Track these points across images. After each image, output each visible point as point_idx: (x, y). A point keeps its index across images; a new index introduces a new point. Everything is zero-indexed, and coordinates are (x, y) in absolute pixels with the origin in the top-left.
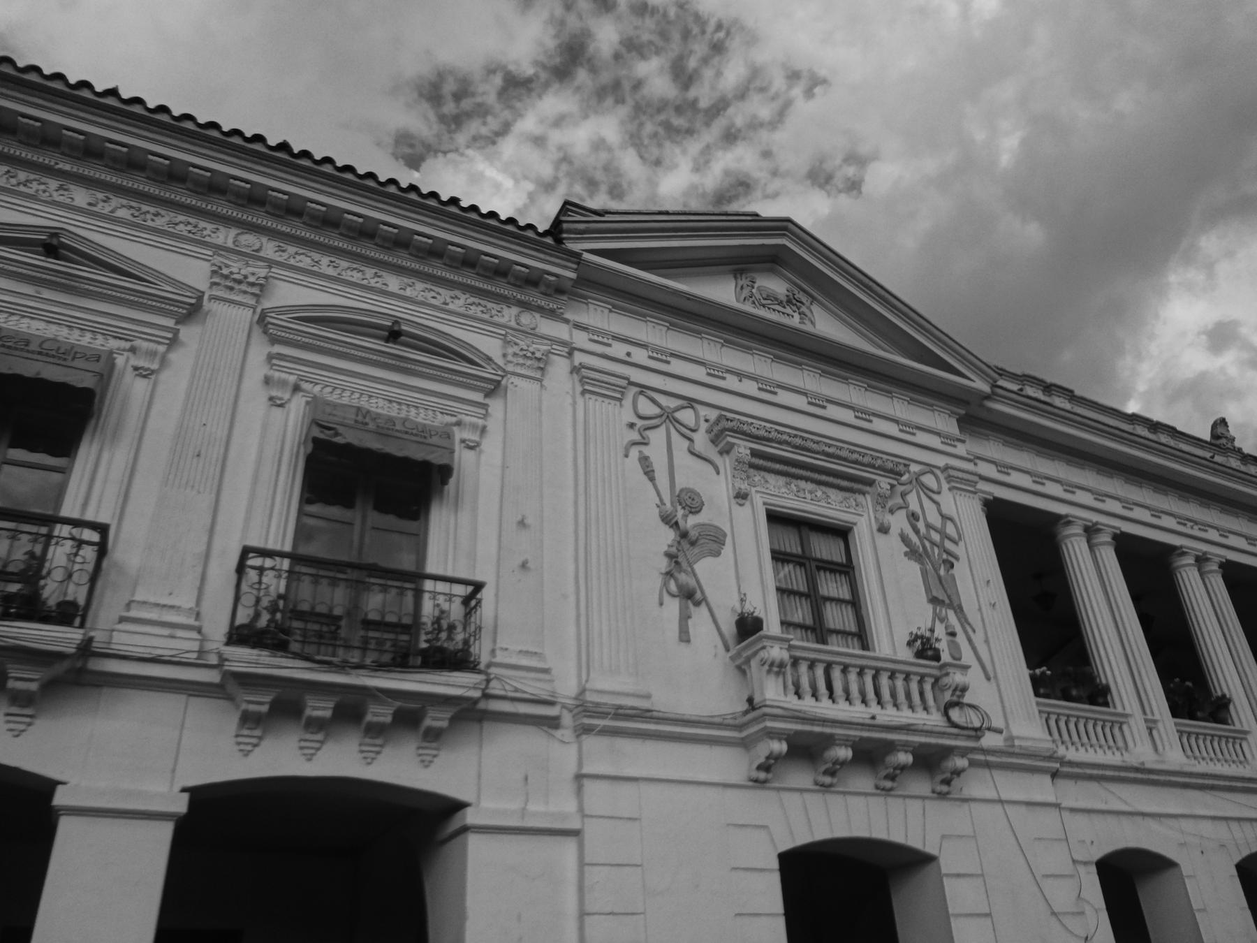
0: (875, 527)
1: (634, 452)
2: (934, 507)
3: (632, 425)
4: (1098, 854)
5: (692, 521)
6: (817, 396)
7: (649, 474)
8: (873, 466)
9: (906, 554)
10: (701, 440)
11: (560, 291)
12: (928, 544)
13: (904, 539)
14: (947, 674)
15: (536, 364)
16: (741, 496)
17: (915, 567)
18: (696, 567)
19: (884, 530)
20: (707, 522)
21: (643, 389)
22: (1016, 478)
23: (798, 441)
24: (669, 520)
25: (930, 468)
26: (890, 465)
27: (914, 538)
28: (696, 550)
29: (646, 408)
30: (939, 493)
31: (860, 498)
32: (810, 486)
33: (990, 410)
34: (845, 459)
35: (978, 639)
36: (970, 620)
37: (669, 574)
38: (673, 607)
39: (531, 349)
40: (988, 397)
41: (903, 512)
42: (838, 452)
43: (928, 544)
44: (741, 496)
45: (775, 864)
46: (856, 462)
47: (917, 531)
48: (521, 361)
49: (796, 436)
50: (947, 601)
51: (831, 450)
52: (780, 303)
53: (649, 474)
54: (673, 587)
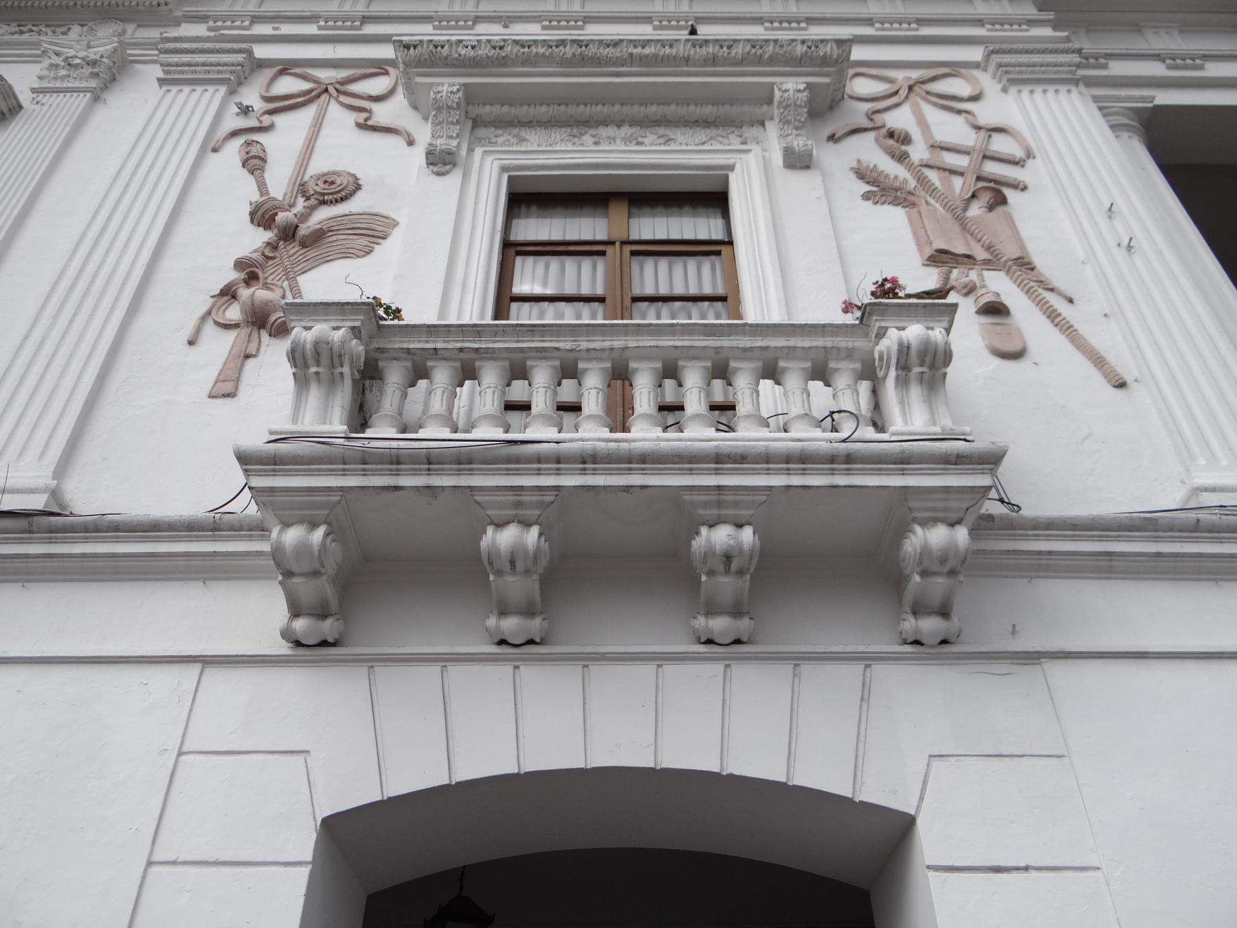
0: (777, 158)
1: (238, 142)
2: (959, 120)
3: (246, 111)
5: (324, 213)
7: (255, 163)
8: (759, 60)
9: (867, 196)
10: (392, 111)
12: (933, 176)
14: (881, 334)
15: (87, 70)
16: (440, 161)
17: (894, 217)
18: (302, 280)
19: (798, 161)
20: (354, 211)
21: (286, 68)
23: (569, 51)
24: (262, 216)
25: (953, 69)
26: (800, 49)
28: (311, 254)
29: (288, 85)
30: (975, 98)
31: (750, 132)
32: (626, 131)
34: (687, 60)
36: (1056, 282)
37: (228, 293)
38: (218, 345)
39: (81, 54)
41: (871, 135)
42: (668, 50)
43: (933, 176)
44: (440, 161)
45: (304, 844)
46: (714, 60)
47: (902, 158)
48: (63, 72)
49: (562, 43)
50: (981, 254)
51: (647, 51)
53: (255, 163)
54: (234, 313)
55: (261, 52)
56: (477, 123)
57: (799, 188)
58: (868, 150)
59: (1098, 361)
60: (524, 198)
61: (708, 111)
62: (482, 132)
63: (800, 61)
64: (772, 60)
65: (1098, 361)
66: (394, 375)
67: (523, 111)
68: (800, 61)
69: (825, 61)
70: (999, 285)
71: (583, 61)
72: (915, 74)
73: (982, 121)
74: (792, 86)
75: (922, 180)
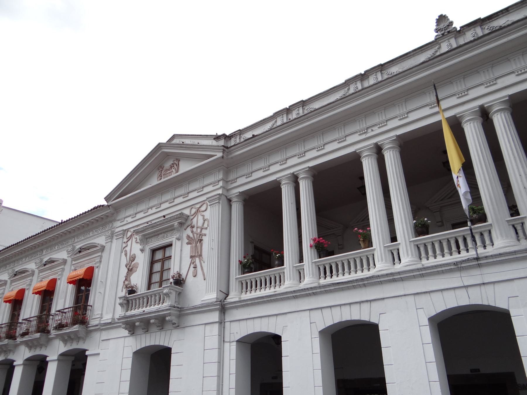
4: (238, 337)
6: (170, 199)
11: (113, 214)
13: (188, 237)
22: (255, 176)
27: (191, 235)
29: (129, 234)
33: (232, 158)
35: (205, 266)
40: (223, 157)
46: (167, 222)
52: (168, 170)
53: (126, 255)
55: (125, 228)
56: (147, 238)
57: (179, 243)
58: (188, 231)
59: (204, 275)
60: (154, 251)
61: (170, 229)
62: (148, 240)
63: (176, 218)
64: (173, 220)
65: (204, 275)
66: (130, 302)
67: (151, 235)
68: (176, 218)
69: (179, 218)
70: (197, 260)
71: (153, 227)
72: (198, 206)
73: (205, 218)
74: (176, 224)
75: (194, 236)
